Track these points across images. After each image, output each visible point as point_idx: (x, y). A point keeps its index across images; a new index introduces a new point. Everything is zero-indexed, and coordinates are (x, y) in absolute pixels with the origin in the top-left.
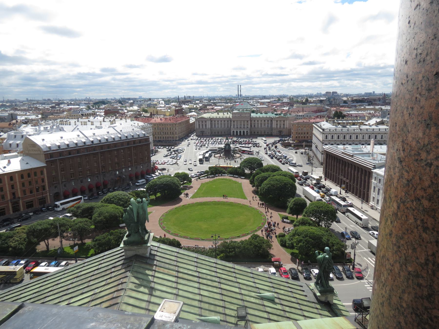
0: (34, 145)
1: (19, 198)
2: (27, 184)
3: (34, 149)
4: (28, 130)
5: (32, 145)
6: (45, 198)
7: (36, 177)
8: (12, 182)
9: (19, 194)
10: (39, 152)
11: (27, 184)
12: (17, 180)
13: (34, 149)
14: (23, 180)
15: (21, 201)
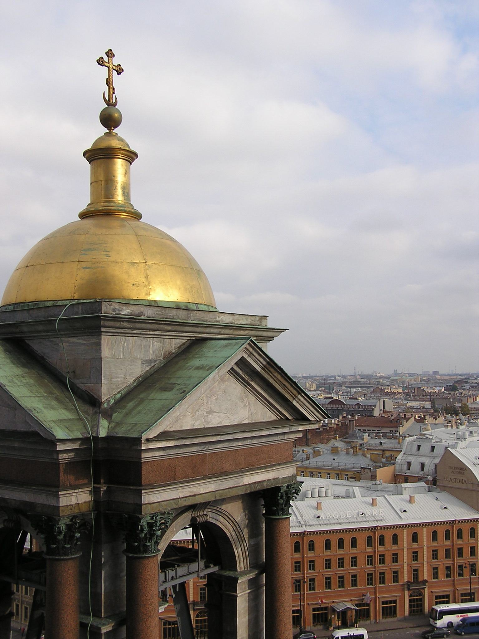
0: (461, 469)
1: (424, 582)
2: (441, 554)
3: (459, 477)
4: (440, 433)
5: (457, 468)
6: (474, 593)
7: (460, 542)
8: (415, 545)
9: (426, 575)
10: (470, 486)
11: (441, 554)
12: (425, 544)
13: (459, 477)
14: (435, 544)
15: (426, 590)
